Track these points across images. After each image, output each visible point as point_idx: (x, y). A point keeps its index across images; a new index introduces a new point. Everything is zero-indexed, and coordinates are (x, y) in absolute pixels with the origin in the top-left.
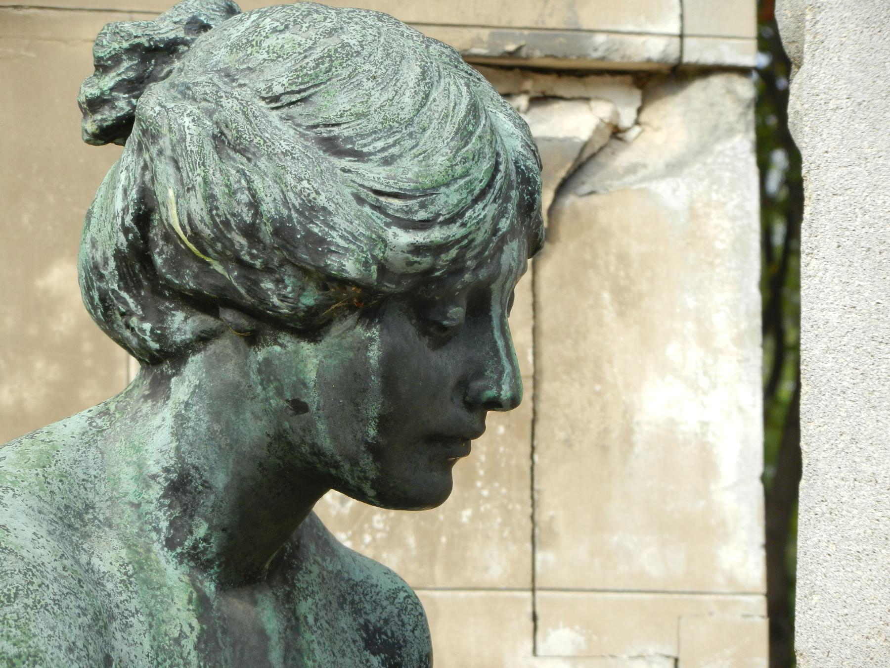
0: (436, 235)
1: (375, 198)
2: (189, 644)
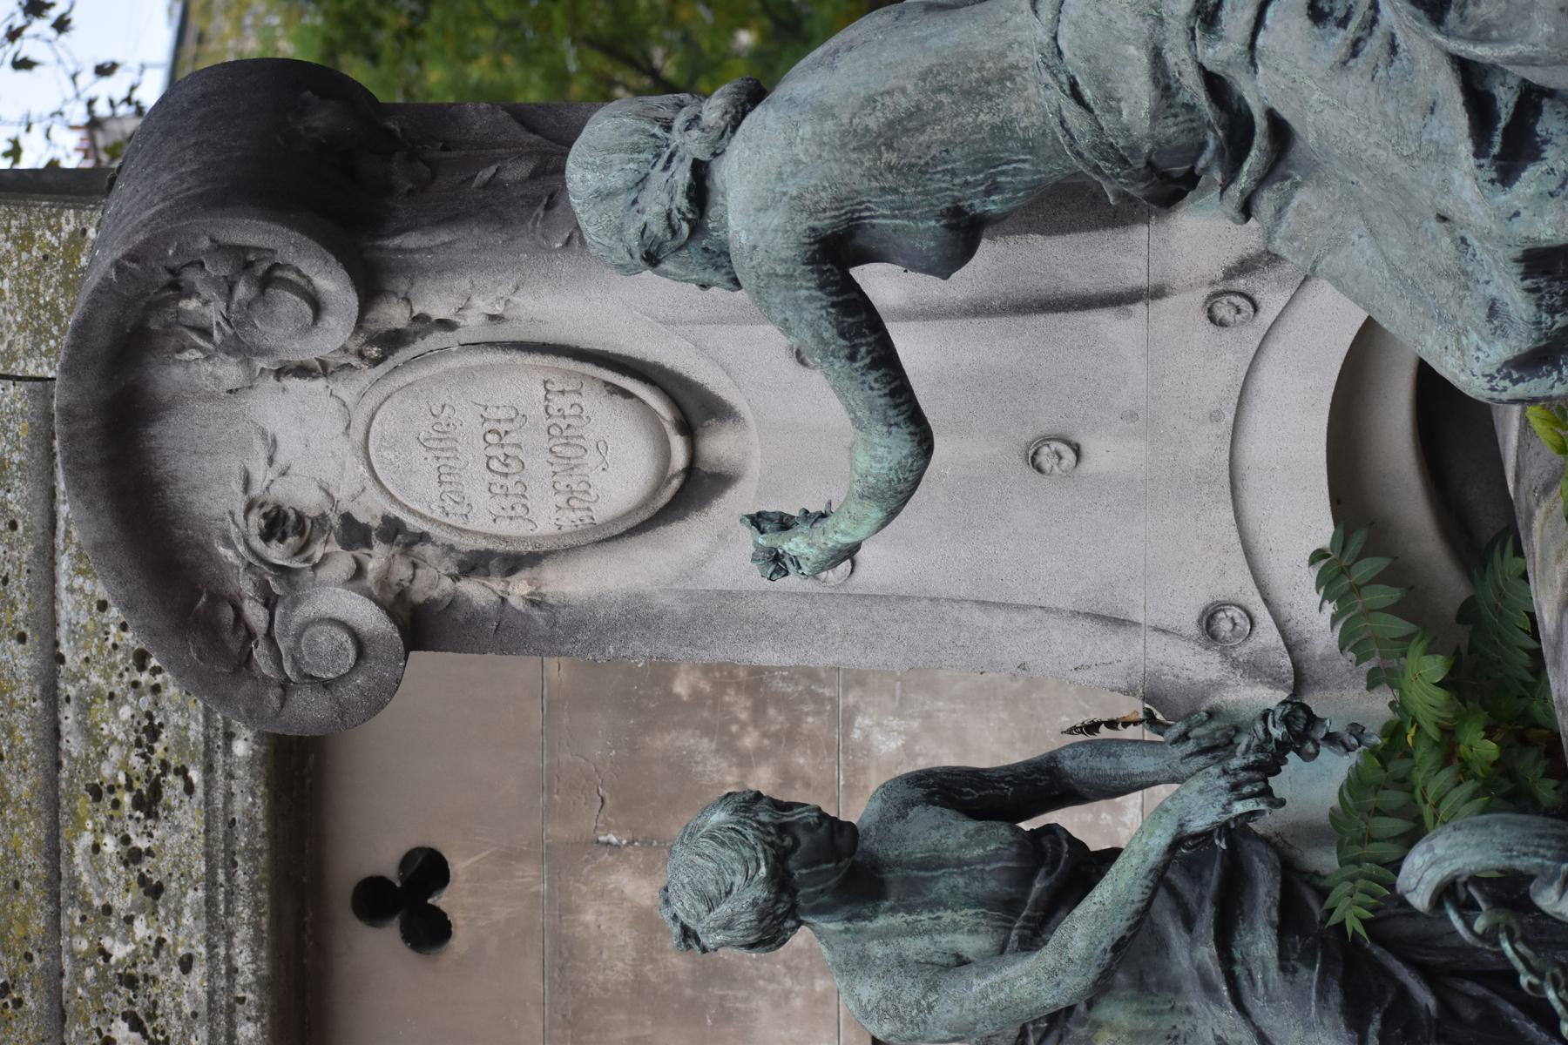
0: (761, 856)
1: (748, 879)
2: (909, 919)
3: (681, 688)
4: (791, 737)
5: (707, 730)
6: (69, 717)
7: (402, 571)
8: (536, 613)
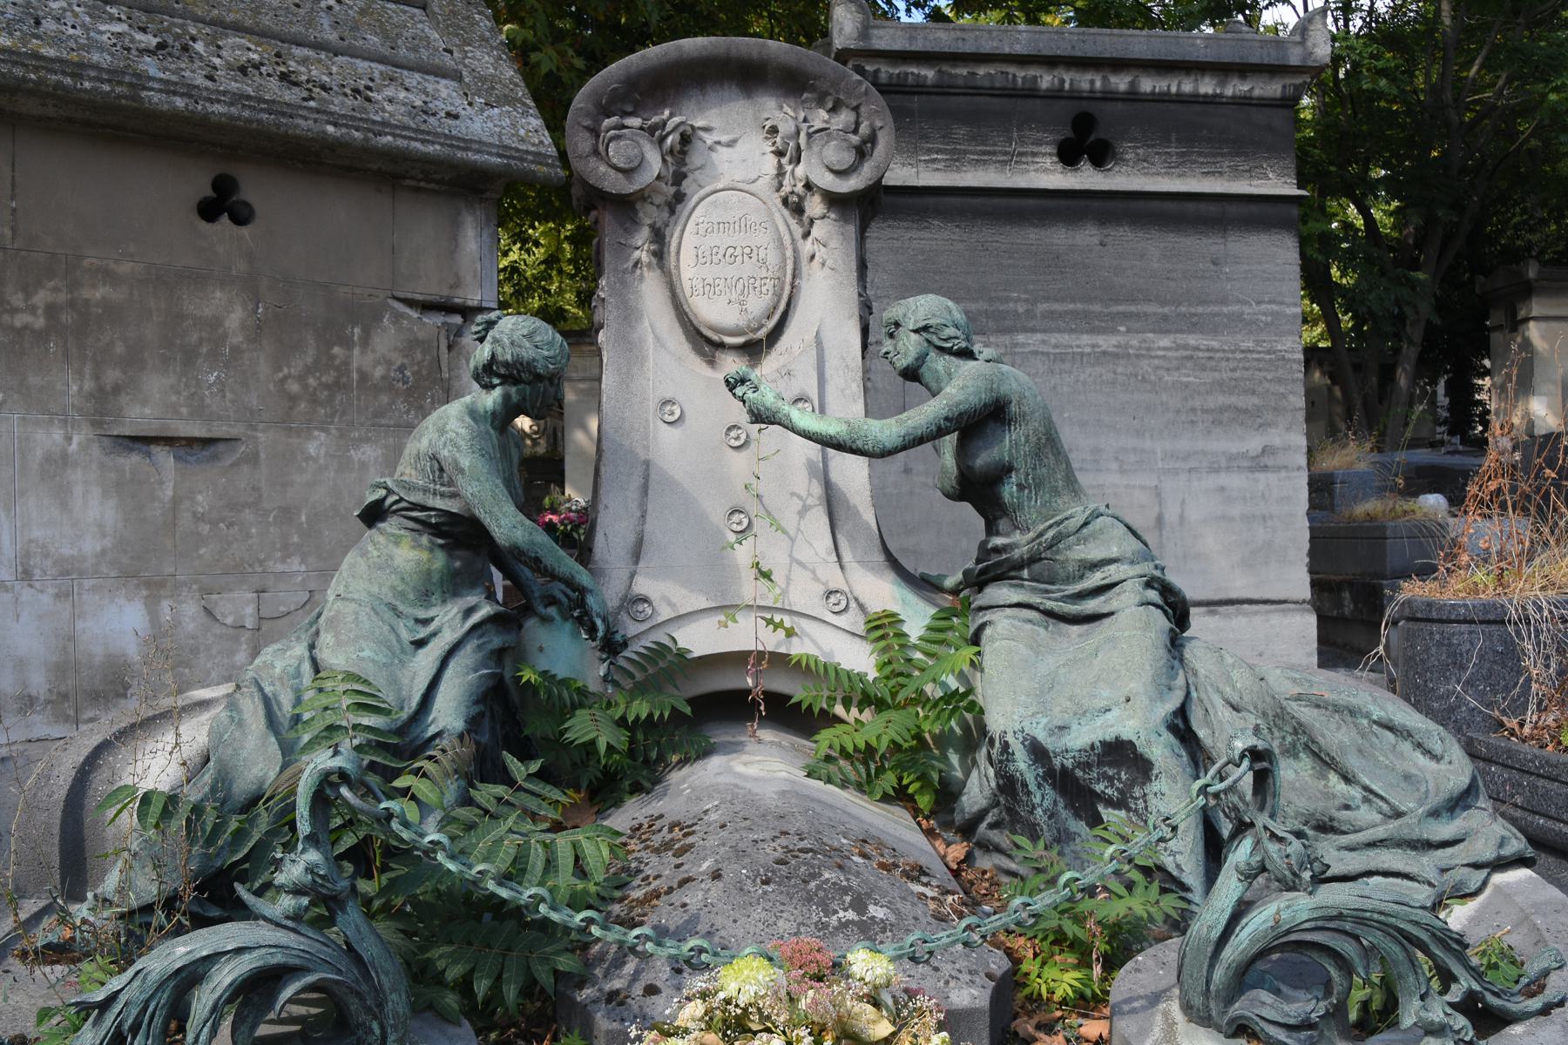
1: (546, 358)
3: (336, 350)
4: (314, 401)
5: (316, 361)
6: (306, 52)
7: (658, 200)
8: (631, 264)
